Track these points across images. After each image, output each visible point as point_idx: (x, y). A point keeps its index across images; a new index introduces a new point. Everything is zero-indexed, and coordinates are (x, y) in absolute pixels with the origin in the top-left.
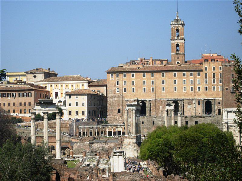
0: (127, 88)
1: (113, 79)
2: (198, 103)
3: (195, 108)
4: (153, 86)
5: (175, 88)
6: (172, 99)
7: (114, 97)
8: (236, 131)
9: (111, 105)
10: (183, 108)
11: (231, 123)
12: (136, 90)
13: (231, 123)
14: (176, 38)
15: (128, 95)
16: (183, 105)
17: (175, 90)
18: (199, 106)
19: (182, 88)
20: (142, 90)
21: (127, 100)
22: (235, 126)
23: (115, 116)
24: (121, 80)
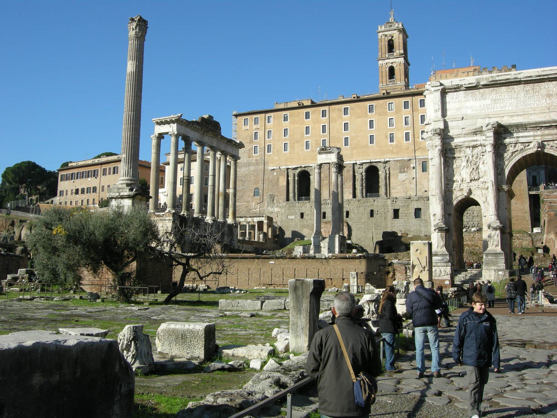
2: (421, 167)
3: (415, 179)
4: (325, 136)
5: (372, 137)
7: (248, 165)
8: (481, 166)
9: (241, 181)
12: (292, 147)
13: (459, 136)
16: (389, 173)
17: (372, 142)
18: (424, 173)
21: (273, 168)
22: (474, 147)
23: (248, 202)
24: (263, 128)
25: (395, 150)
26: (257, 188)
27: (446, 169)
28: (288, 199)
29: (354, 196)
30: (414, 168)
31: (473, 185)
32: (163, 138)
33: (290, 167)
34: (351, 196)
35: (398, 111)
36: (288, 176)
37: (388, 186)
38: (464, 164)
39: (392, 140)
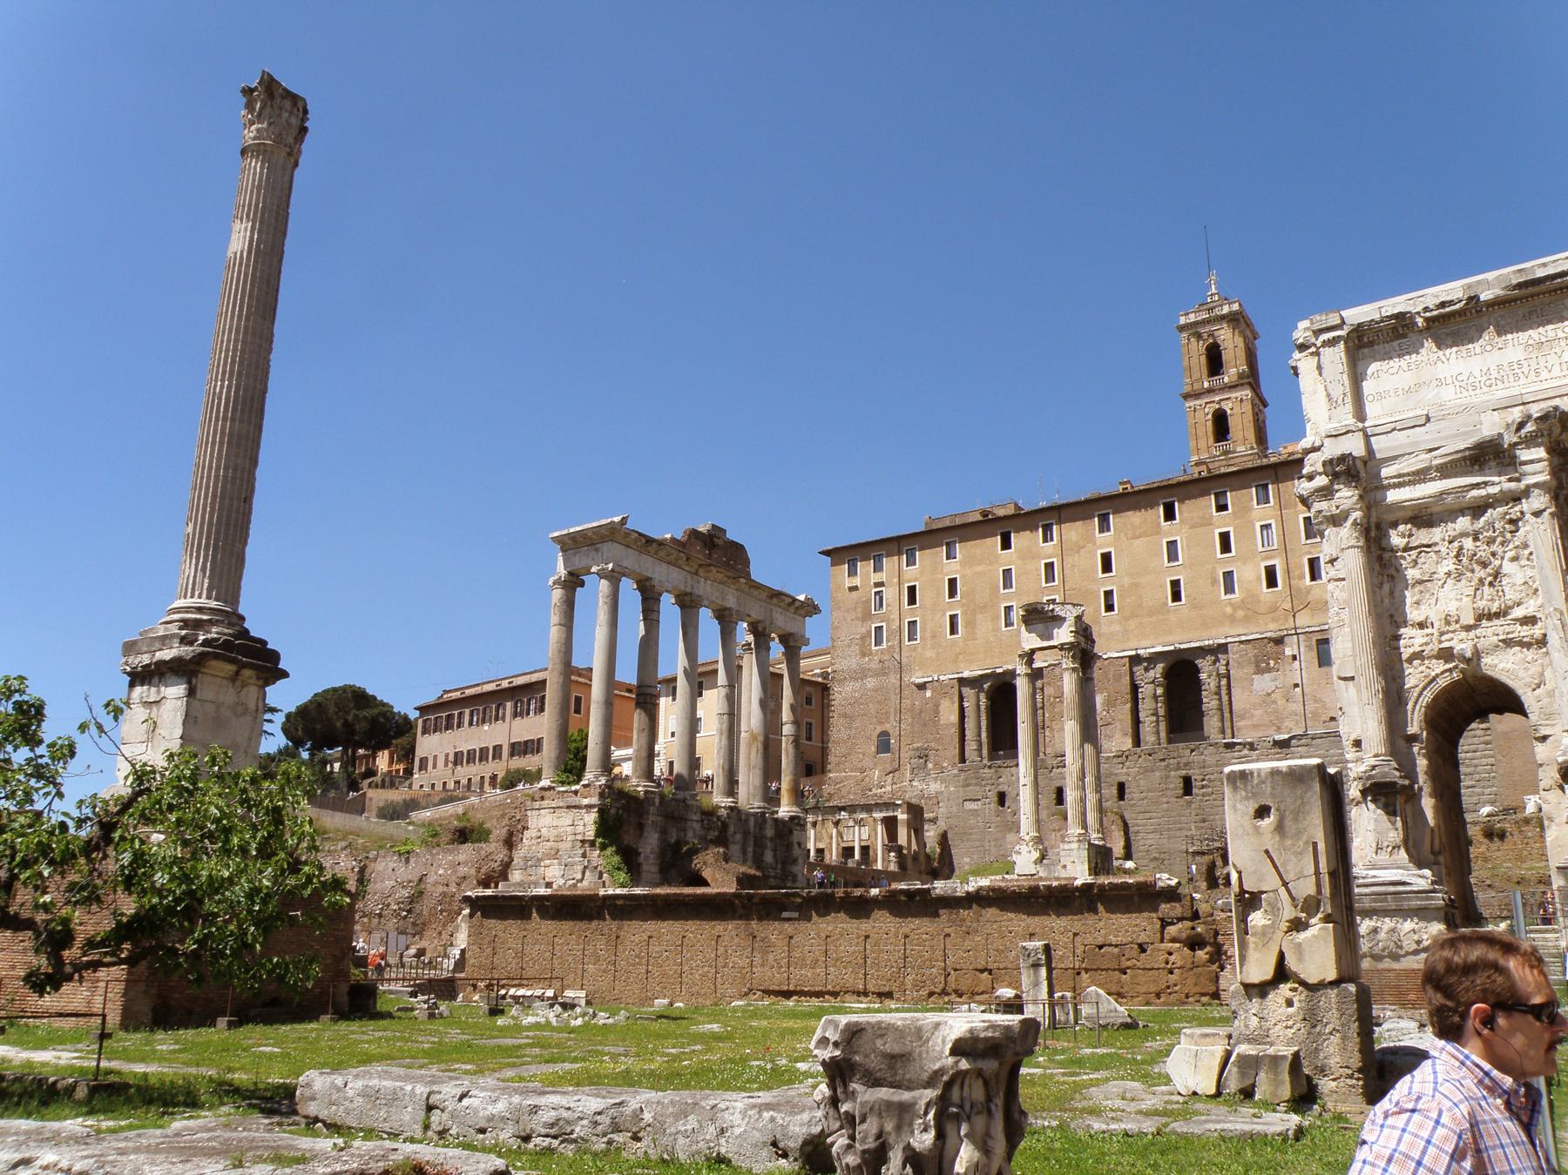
0: (923, 622)
1: (857, 581)
2: (1315, 654)
3: (1298, 690)
5: (1175, 584)
6: (1159, 649)
7: (861, 674)
8: (1508, 567)
9: (845, 716)
10: (1225, 698)
11: (1420, 476)
13: (1420, 476)
14: (1206, 385)
15: (930, 654)
17: (1176, 596)
18: (1324, 669)
19: (1214, 582)
20: (998, 617)
22: (1478, 509)
25: (1240, 613)
26: (885, 734)
27: (1386, 587)
28: (963, 760)
29: (1137, 742)
30: (1294, 658)
31: (1491, 632)
32: (582, 584)
33: (966, 674)
34: (1128, 743)
35: (1245, 510)
36: (961, 699)
37: (1227, 711)
38: (1449, 565)
39: (1229, 588)
